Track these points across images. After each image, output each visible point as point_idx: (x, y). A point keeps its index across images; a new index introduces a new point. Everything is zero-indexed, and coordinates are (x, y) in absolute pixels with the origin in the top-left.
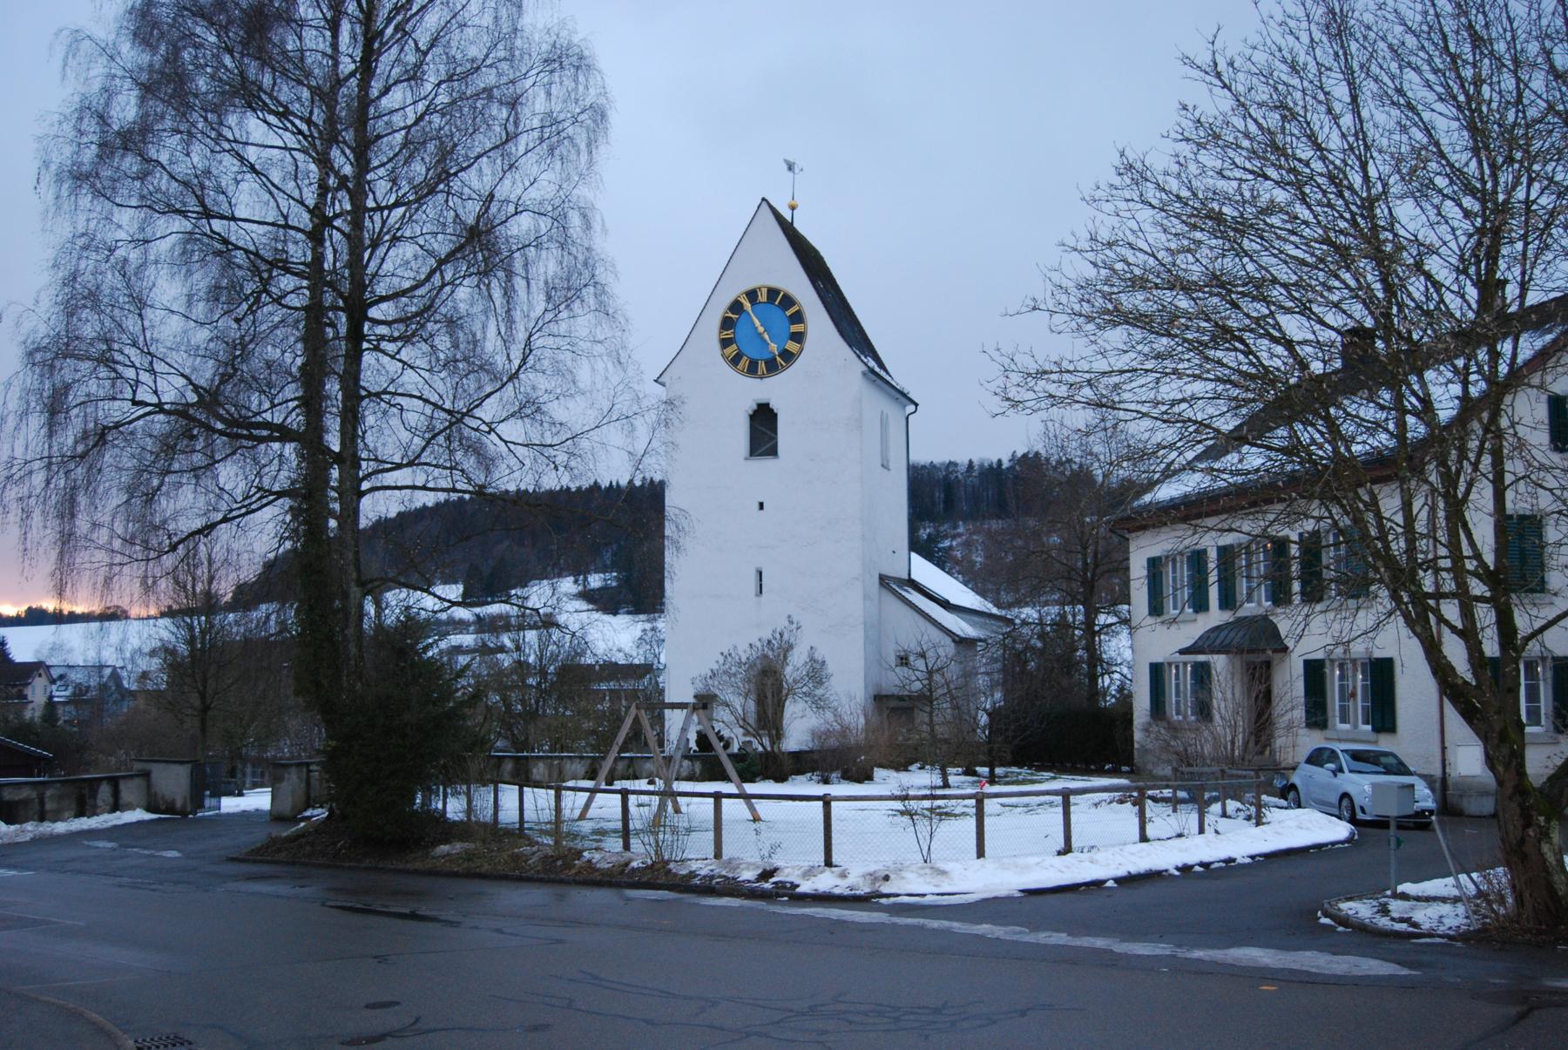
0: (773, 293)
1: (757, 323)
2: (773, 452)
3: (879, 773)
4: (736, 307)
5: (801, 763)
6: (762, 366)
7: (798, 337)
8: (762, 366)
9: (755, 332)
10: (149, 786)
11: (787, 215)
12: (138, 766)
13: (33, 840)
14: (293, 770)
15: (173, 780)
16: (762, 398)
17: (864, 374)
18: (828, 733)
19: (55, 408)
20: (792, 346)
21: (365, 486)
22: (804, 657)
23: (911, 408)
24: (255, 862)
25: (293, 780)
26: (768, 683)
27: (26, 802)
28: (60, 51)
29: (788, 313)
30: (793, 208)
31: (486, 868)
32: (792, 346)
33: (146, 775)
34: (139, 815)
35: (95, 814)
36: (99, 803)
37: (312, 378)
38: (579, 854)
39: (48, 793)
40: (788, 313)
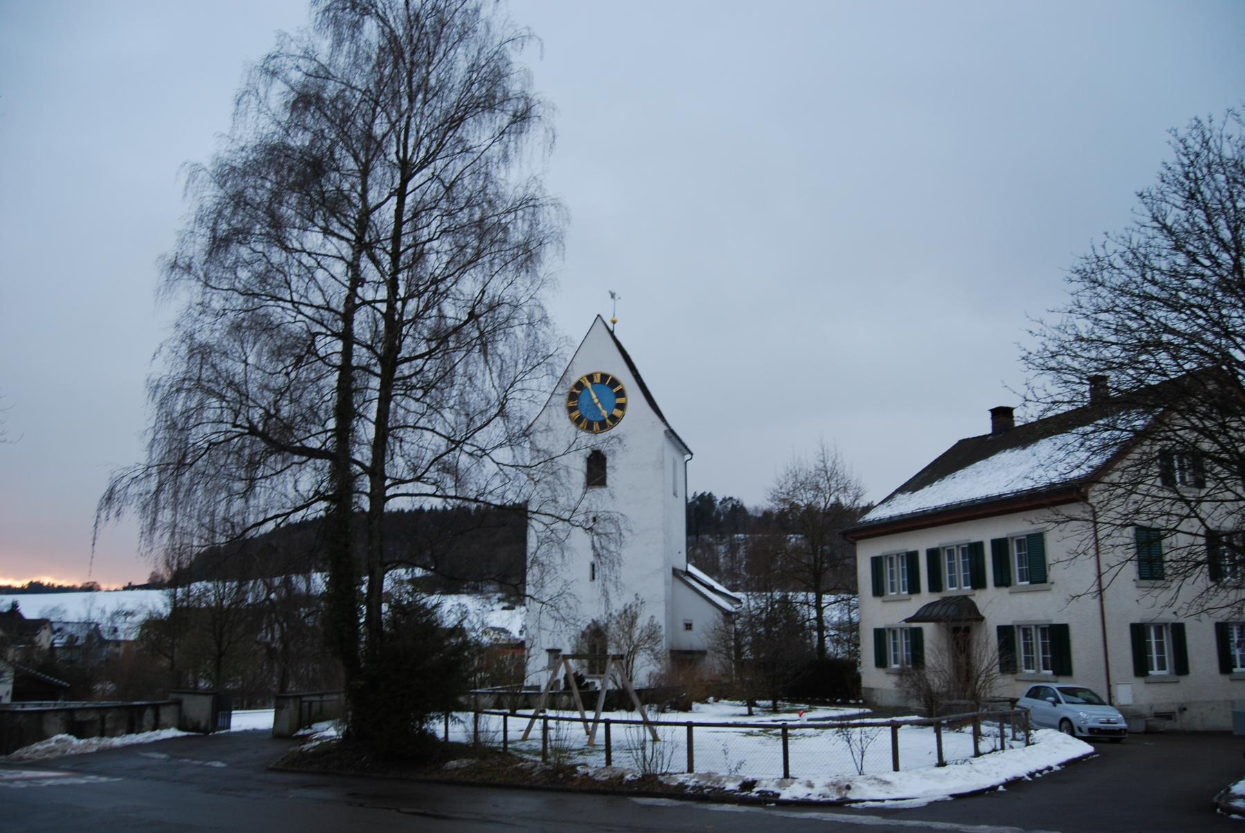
0: (604, 377)
1: (594, 396)
2: (602, 483)
3: (695, 705)
6: (596, 426)
7: (622, 407)
10: (180, 711)
12: (172, 696)
14: (291, 701)
15: (198, 708)
20: (617, 412)
21: (388, 493)
22: (646, 624)
23: (688, 456)
24: (293, 772)
26: (595, 643)
27: (91, 722)
28: (184, 177)
30: (614, 322)
31: (498, 780)
32: (617, 412)
33: (179, 703)
35: (140, 730)
36: (145, 723)
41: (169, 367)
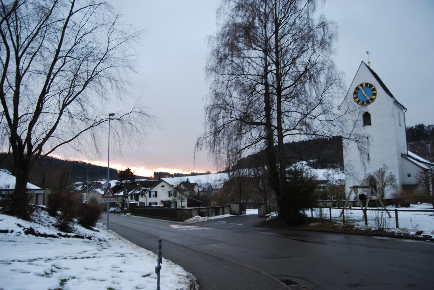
0: (367, 84)
1: (363, 92)
2: (370, 124)
3: (411, 205)
4: (357, 89)
5: (389, 202)
6: (365, 103)
7: (375, 95)
8: (365, 103)
9: (363, 94)
10: (230, 209)
11: (368, 65)
12: (227, 204)
13: (207, 221)
14: (263, 205)
15: (235, 207)
16: (365, 110)
17: (394, 102)
18: (397, 195)
19: (214, 120)
20: (373, 97)
21: (284, 134)
22: (389, 175)
23: (405, 110)
24: (261, 227)
25: (263, 207)
26: (371, 182)
27: (205, 212)
28: (207, 41)
29: (371, 89)
30: (369, 63)
31: (327, 229)
32: (373, 97)
33: (229, 206)
34: (228, 215)
35: (219, 215)
36: (220, 212)
37: (268, 109)
38: (353, 226)
39: (209, 210)
40: (371, 89)
41: (209, 102)
